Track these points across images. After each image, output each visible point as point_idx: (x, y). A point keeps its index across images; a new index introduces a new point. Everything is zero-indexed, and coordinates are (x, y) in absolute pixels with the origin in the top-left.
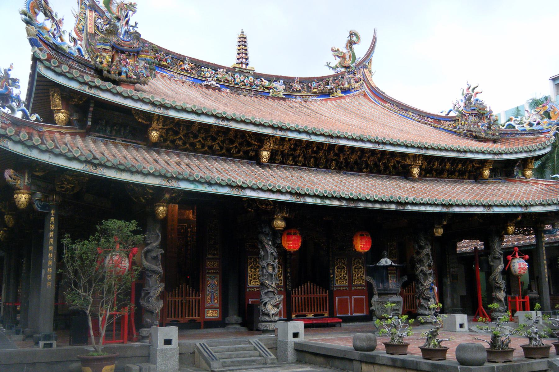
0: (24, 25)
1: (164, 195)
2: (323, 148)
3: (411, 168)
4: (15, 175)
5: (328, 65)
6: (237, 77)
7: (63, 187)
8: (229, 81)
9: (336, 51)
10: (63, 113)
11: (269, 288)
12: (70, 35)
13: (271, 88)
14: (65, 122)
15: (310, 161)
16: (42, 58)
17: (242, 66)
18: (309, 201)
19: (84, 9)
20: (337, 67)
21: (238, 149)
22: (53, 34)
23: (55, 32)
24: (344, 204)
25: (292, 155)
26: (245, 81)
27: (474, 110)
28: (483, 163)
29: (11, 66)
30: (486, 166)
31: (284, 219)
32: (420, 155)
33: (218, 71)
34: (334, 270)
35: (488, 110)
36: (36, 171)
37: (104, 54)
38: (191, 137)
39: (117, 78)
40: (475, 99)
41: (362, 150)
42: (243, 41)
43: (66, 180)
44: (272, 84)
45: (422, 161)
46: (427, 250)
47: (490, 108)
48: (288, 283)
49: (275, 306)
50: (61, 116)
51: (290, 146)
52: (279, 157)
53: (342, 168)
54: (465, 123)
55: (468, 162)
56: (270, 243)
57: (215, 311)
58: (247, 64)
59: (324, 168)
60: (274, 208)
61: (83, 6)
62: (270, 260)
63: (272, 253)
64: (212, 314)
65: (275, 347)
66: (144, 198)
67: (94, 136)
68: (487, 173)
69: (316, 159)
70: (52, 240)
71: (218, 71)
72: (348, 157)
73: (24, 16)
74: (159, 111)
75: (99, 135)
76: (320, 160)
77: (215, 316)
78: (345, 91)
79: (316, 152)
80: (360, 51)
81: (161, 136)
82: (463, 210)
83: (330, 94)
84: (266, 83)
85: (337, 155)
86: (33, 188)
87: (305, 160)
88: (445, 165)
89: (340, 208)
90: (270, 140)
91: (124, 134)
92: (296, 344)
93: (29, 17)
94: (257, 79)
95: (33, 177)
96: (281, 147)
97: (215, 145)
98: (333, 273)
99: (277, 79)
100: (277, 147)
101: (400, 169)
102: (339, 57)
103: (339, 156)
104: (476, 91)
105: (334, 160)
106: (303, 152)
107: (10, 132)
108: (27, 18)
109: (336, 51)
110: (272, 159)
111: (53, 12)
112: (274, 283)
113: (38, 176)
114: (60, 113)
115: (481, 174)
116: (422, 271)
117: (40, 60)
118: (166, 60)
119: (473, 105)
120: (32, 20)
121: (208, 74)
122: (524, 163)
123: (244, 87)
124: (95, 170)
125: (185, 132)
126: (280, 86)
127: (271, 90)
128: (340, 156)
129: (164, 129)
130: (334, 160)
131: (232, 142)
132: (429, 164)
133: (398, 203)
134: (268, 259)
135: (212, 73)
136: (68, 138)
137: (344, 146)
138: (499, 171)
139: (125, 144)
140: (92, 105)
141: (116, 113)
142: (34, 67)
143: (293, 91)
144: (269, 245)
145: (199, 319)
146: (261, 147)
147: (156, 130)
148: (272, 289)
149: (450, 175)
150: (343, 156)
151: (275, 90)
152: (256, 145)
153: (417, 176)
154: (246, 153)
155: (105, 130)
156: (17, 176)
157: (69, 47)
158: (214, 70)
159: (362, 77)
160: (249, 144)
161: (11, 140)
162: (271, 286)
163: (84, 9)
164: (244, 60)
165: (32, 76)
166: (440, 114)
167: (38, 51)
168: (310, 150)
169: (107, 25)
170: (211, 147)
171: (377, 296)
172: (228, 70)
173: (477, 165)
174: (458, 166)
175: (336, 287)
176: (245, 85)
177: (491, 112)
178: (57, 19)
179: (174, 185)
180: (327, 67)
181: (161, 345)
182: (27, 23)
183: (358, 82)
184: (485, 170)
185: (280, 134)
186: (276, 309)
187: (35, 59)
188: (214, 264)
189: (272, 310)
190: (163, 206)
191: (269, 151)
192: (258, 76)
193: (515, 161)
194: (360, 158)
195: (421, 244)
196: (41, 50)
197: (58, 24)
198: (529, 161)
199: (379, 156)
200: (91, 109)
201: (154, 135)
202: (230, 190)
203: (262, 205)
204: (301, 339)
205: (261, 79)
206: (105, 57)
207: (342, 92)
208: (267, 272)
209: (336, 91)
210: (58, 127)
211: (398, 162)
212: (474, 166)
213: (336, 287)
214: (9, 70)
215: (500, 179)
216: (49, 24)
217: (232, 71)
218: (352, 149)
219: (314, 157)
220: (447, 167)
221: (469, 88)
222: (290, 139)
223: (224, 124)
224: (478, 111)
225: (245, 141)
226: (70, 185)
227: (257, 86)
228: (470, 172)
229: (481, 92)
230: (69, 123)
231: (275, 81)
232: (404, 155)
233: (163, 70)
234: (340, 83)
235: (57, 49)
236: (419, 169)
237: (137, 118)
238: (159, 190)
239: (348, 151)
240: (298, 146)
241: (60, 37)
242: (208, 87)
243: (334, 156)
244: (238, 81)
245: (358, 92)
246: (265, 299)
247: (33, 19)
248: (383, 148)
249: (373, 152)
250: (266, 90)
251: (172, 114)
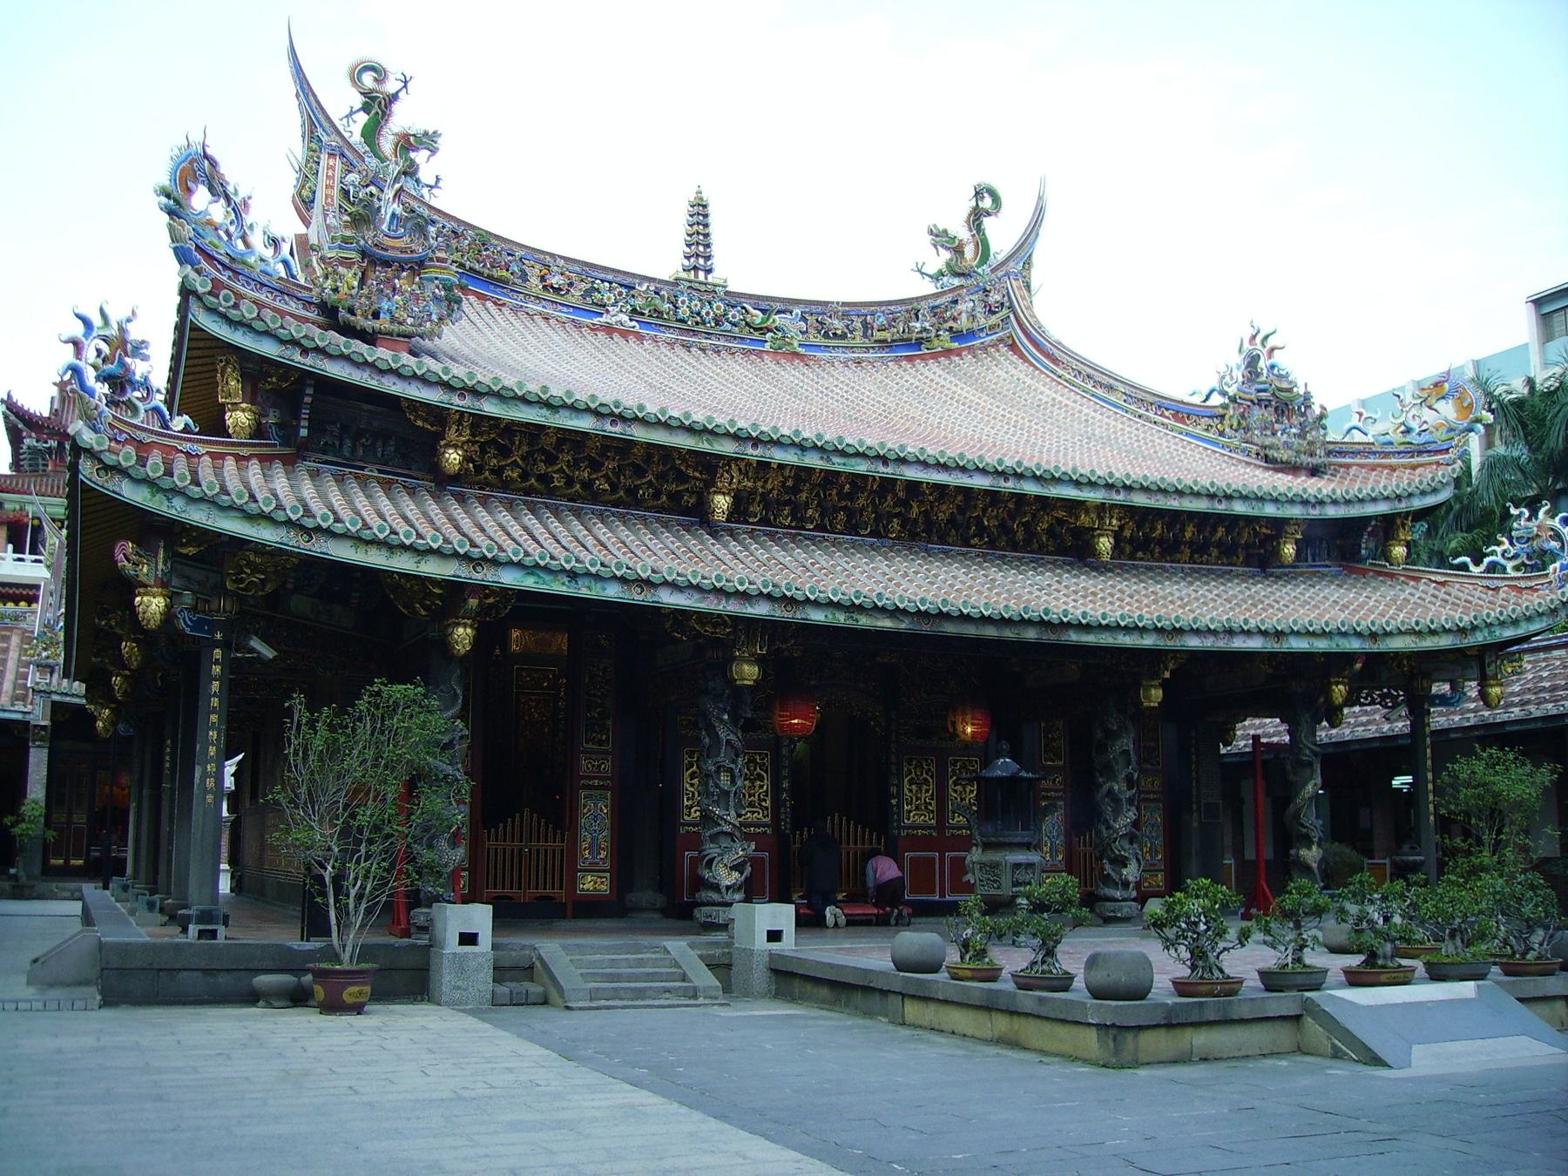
0: (166, 218)
1: (466, 600)
2: (866, 486)
3: (1093, 536)
4: (137, 554)
6: (683, 302)
7: (242, 581)
8: (662, 313)
9: (940, 237)
10: (243, 410)
11: (720, 825)
12: (265, 233)
13: (770, 330)
14: (248, 431)
15: (835, 518)
16: (201, 290)
17: (696, 276)
18: (817, 616)
19: (314, 151)
20: (941, 274)
21: (655, 488)
22: (227, 232)
23: (232, 229)
25: (787, 503)
26: (703, 312)
27: (1265, 391)
28: (1279, 525)
29: (133, 313)
30: (1286, 532)
31: (759, 661)
32: (1113, 506)
33: (634, 288)
34: (900, 787)
35: (1302, 392)
36: (183, 545)
37: (341, 269)
38: (541, 461)
39: (369, 324)
40: (1269, 363)
41: (967, 492)
42: (700, 213)
43: (249, 564)
44: (771, 320)
45: (1119, 519)
46: (1126, 743)
47: (1306, 385)
48: (783, 817)
49: (734, 868)
50: (239, 418)
51: (784, 483)
52: (755, 508)
53: (918, 534)
54: (1239, 423)
55: (1241, 523)
56: (726, 717)
57: (602, 878)
58: (709, 271)
59: (870, 535)
60: (734, 632)
61: (314, 146)
62: (723, 758)
63: (728, 742)
64: (591, 884)
65: (726, 962)
66: (425, 607)
67: (314, 461)
68: (1289, 550)
69: (850, 513)
70: (216, 699)
71: (634, 288)
72: (932, 508)
73: (164, 200)
74: (461, 403)
75: (325, 457)
76: (861, 515)
77: (599, 890)
78: (957, 335)
79: (851, 497)
80: (1002, 235)
81: (467, 459)
83: (922, 343)
84: (758, 317)
85: (905, 503)
86: (175, 582)
87: (822, 515)
88: (1183, 530)
90: (730, 467)
91: (383, 455)
92: (771, 955)
93: (177, 202)
94: (733, 307)
95: (173, 556)
96: (759, 484)
97: (597, 479)
98: (900, 795)
99: (786, 305)
100: (750, 484)
101: (1069, 541)
102: (947, 249)
103: (908, 506)
104: (1270, 343)
105: (897, 515)
106: (818, 495)
107: (126, 459)
108: (172, 202)
109: (940, 237)
110: (739, 512)
111: (227, 183)
112: (733, 813)
113: (186, 556)
114: (236, 410)
115: (1276, 553)
116: (1110, 792)
117: (195, 293)
119: (1263, 378)
120: (181, 206)
121: (609, 298)
122: (1387, 526)
123: (701, 328)
124: (308, 542)
125: (525, 448)
127: (769, 335)
128: (911, 507)
129: (478, 442)
130: (897, 515)
131: (639, 472)
132: (1139, 527)
133: (1043, 624)
134: (718, 755)
135: (620, 294)
136: (254, 470)
137: (922, 483)
138: (1324, 545)
139: (384, 479)
140: (310, 391)
141: (366, 407)
142: (183, 310)
143: (828, 337)
144: (722, 721)
145: (560, 894)
146: (710, 484)
147: (455, 447)
148: (727, 828)
149: (1196, 556)
150: (918, 507)
151: (780, 334)
152: (696, 478)
153: (1106, 558)
154: (675, 497)
155: (341, 446)
156: (140, 556)
157: (262, 260)
158: (626, 286)
159: (1006, 298)
160: (682, 478)
161: (129, 476)
162: (725, 820)
163: (314, 151)
164: (701, 261)
165: (179, 328)
166: (1187, 399)
167: (193, 275)
168: (835, 492)
169: (367, 186)
170: (587, 485)
171: (980, 850)
173: (1264, 530)
174: (1217, 532)
175: (905, 828)
177: (1307, 397)
178: (237, 200)
179: (486, 576)
180: (918, 274)
181: (452, 945)
182: (171, 213)
183: (994, 313)
184: (1285, 543)
185: (753, 453)
186: (736, 874)
187: (186, 292)
188: (599, 766)
189: (727, 878)
190: (465, 626)
191: (729, 494)
192: (734, 300)
193: (1363, 521)
194: (961, 510)
195: (1110, 726)
196: (199, 272)
197: (238, 210)
198: (1399, 521)
199: (1011, 505)
200: (308, 400)
201: (453, 457)
202: (620, 589)
203: (703, 625)
204: (788, 944)
205: (744, 308)
206: (341, 277)
207: (953, 339)
208: (717, 786)
209: (938, 336)
210: (233, 444)
211: (1060, 522)
212: (1256, 534)
213: (905, 828)
214: (129, 320)
215: (1327, 566)
216: (218, 212)
218: (940, 489)
219: (845, 508)
220: (1188, 535)
221: (1254, 337)
222: (781, 466)
223: (617, 430)
224: (1273, 394)
225: (670, 469)
226: (257, 575)
227: (734, 325)
228: (1247, 546)
229: (1281, 346)
230: (258, 431)
231: (779, 312)
232: (1074, 506)
233: (498, 290)
234: (948, 313)
235: (234, 266)
236: (1112, 540)
237: (412, 417)
238: (455, 590)
239: (931, 494)
240: (805, 481)
241: (244, 238)
242: (609, 329)
243: (895, 505)
244: (684, 312)
245: (994, 337)
246: (712, 850)
247: (183, 202)
248: (1018, 486)
250: (756, 333)
251: (490, 408)
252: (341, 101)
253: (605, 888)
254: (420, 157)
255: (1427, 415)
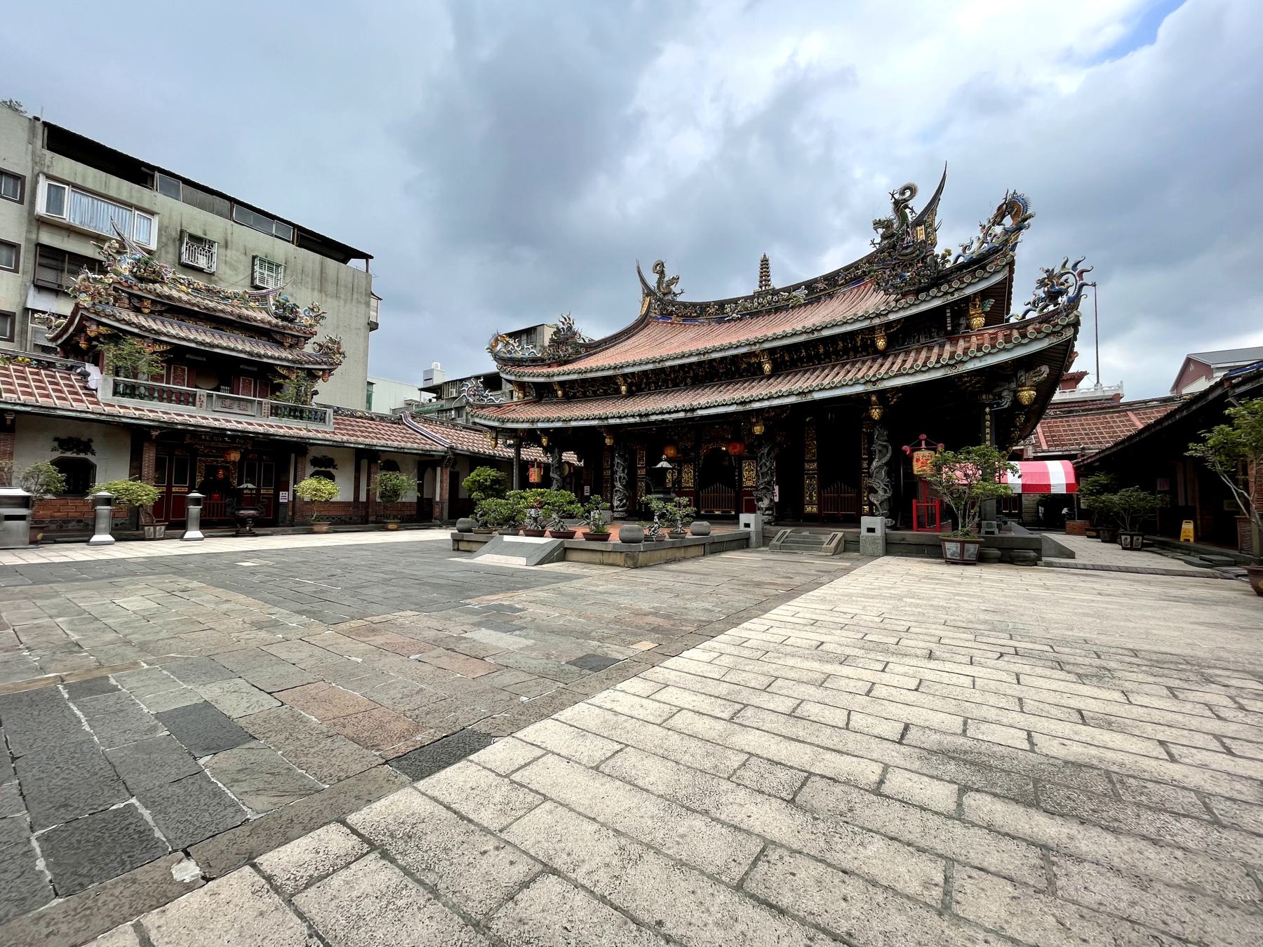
5: (873, 243)
9: (878, 224)
18: (612, 421)
20: (881, 241)
24: (637, 419)
28: (871, 330)
42: (765, 263)
52: (643, 386)
80: (918, 205)
82: (766, 404)
89: (635, 424)
99: (797, 287)
118: (696, 312)
126: (801, 294)
172: (746, 299)
176: (764, 306)
192: (775, 292)
217: (751, 298)
220: (821, 351)
242: (729, 321)
249: (700, 364)
252: (652, 280)
253: (815, 510)
254: (672, 287)
255: (998, 230)
